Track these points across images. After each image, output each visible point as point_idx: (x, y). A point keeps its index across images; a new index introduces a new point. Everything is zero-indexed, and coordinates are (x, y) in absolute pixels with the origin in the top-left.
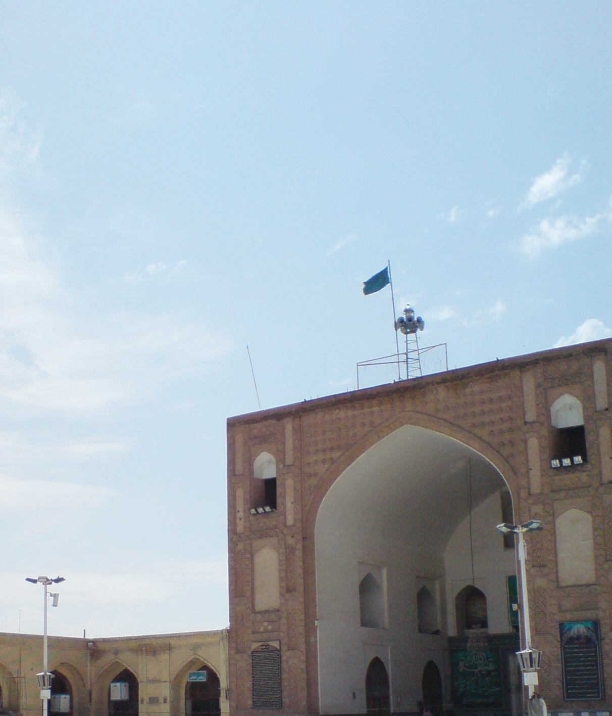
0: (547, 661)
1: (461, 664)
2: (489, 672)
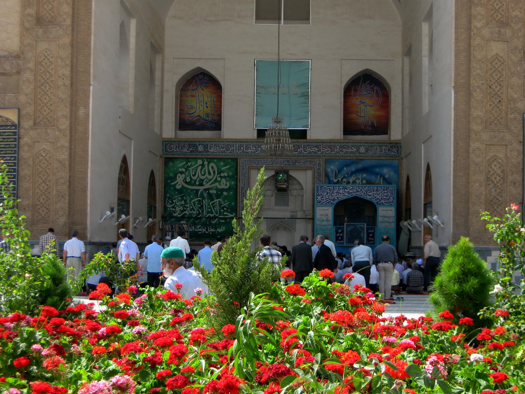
0: (499, 172)
1: (180, 179)
2: (220, 193)
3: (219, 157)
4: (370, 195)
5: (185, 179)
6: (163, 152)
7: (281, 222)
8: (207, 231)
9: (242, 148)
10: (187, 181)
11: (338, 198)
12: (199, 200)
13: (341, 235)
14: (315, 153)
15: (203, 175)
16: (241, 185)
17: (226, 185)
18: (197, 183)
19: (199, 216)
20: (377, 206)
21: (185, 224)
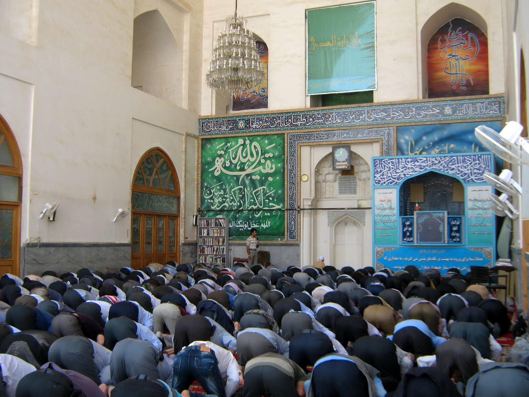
1: (219, 164)
3: (262, 133)
4: (453, 169)
5: (225, 163)
6: (200, 132)
7: (346, 214)
8: (250, 227)
9: (290, 120)
10: (227, 165)
11: (404, 175)
12: (241, 188)
13: (410, 229)
14: (384, 119)
15: (245, 157)
16: (288, 167)
17: (272, 168)
18: (238, 168)
19: (241, 209)
20: (464, 185)
21: (221, 219)
